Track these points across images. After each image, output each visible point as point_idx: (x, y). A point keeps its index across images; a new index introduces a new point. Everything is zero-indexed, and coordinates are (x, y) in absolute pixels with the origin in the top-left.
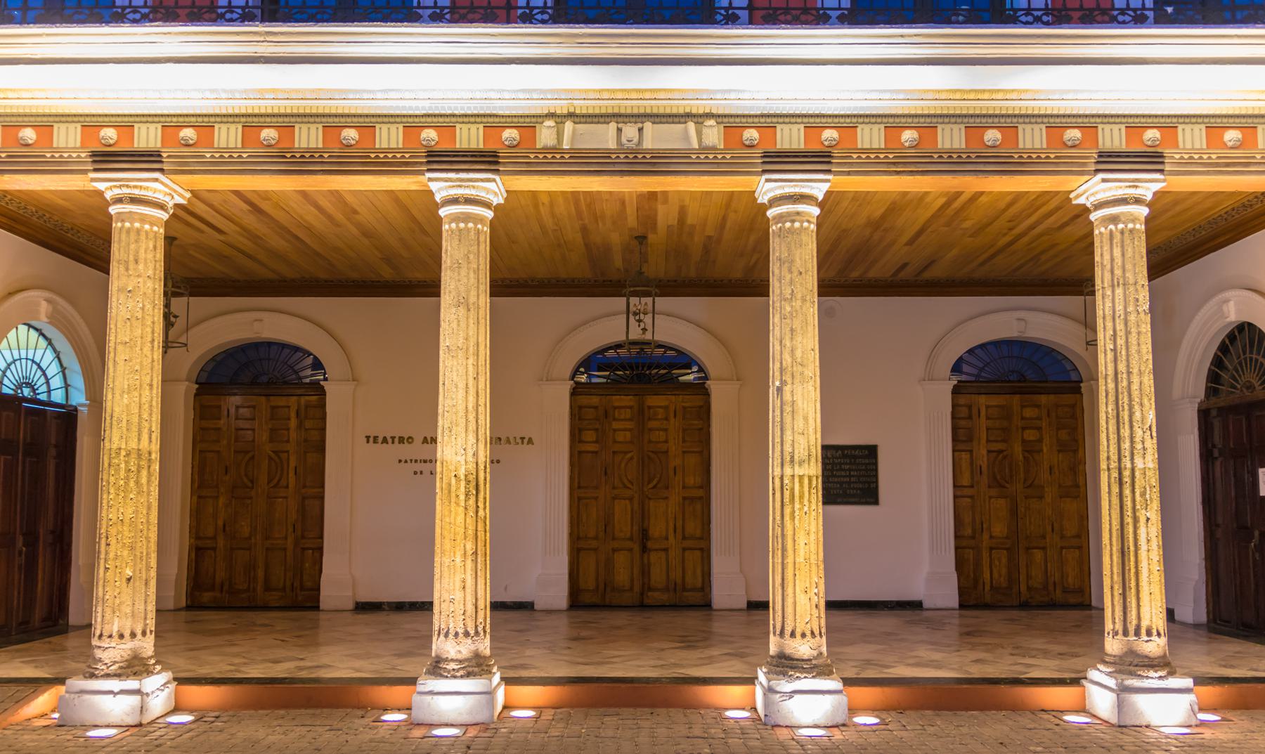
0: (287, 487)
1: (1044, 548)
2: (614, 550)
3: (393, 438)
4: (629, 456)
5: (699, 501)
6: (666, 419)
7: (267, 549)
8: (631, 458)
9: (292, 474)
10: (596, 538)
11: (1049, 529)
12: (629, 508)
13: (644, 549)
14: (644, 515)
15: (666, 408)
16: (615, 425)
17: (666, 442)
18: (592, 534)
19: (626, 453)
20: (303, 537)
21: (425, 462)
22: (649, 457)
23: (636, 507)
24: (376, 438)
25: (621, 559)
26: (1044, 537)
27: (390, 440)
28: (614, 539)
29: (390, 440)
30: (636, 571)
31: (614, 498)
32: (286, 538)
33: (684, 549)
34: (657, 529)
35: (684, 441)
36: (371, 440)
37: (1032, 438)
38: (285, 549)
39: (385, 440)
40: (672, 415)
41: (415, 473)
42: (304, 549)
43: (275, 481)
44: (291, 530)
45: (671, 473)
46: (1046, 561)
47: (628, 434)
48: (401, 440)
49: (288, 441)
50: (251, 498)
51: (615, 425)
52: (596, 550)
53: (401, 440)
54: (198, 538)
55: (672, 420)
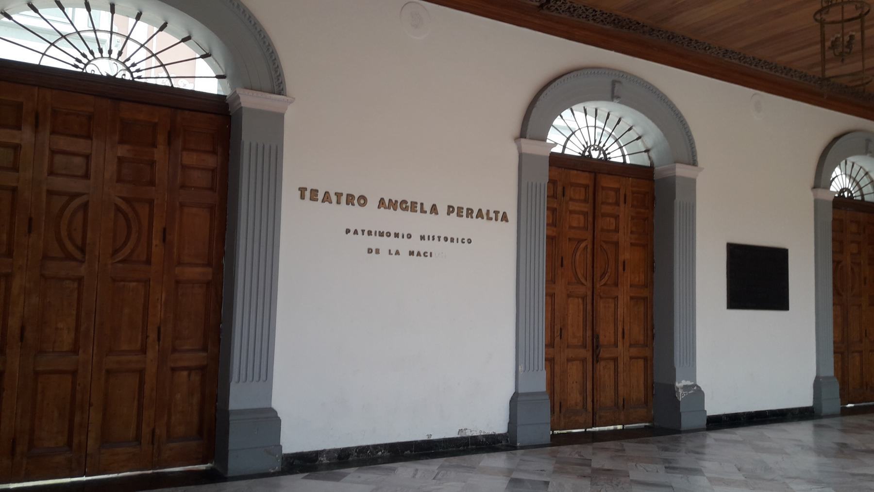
0: (148, 262)
1: (861, 352)
2: (568, 360)
3: (339, 195)
4: (583, 245)
6: (617, 204)
7: (108, 372)
11: (864, 335)
13: (596, 358)
15: (617, 191)
16: (573, 206)
17: (617, 230)
19: (580, 241)
20: (174, 350)
21: (381, 234)
23: (589, 307)
26: (861, 341)
27: (334, 199)
31: (569, 296)
32: (144, 351)
34: (606, 335)
35: (632, 232)
36: (308, 194)
38: (141, 372)
39: (327, 198)
41: (370, 251)
42: (173, 370)
43: (126, 251)
44: (153, 336)
45: (621, 268)
47: (582, 217)
48: (350, 199)
49: (152, 183)
53: (350, 199)
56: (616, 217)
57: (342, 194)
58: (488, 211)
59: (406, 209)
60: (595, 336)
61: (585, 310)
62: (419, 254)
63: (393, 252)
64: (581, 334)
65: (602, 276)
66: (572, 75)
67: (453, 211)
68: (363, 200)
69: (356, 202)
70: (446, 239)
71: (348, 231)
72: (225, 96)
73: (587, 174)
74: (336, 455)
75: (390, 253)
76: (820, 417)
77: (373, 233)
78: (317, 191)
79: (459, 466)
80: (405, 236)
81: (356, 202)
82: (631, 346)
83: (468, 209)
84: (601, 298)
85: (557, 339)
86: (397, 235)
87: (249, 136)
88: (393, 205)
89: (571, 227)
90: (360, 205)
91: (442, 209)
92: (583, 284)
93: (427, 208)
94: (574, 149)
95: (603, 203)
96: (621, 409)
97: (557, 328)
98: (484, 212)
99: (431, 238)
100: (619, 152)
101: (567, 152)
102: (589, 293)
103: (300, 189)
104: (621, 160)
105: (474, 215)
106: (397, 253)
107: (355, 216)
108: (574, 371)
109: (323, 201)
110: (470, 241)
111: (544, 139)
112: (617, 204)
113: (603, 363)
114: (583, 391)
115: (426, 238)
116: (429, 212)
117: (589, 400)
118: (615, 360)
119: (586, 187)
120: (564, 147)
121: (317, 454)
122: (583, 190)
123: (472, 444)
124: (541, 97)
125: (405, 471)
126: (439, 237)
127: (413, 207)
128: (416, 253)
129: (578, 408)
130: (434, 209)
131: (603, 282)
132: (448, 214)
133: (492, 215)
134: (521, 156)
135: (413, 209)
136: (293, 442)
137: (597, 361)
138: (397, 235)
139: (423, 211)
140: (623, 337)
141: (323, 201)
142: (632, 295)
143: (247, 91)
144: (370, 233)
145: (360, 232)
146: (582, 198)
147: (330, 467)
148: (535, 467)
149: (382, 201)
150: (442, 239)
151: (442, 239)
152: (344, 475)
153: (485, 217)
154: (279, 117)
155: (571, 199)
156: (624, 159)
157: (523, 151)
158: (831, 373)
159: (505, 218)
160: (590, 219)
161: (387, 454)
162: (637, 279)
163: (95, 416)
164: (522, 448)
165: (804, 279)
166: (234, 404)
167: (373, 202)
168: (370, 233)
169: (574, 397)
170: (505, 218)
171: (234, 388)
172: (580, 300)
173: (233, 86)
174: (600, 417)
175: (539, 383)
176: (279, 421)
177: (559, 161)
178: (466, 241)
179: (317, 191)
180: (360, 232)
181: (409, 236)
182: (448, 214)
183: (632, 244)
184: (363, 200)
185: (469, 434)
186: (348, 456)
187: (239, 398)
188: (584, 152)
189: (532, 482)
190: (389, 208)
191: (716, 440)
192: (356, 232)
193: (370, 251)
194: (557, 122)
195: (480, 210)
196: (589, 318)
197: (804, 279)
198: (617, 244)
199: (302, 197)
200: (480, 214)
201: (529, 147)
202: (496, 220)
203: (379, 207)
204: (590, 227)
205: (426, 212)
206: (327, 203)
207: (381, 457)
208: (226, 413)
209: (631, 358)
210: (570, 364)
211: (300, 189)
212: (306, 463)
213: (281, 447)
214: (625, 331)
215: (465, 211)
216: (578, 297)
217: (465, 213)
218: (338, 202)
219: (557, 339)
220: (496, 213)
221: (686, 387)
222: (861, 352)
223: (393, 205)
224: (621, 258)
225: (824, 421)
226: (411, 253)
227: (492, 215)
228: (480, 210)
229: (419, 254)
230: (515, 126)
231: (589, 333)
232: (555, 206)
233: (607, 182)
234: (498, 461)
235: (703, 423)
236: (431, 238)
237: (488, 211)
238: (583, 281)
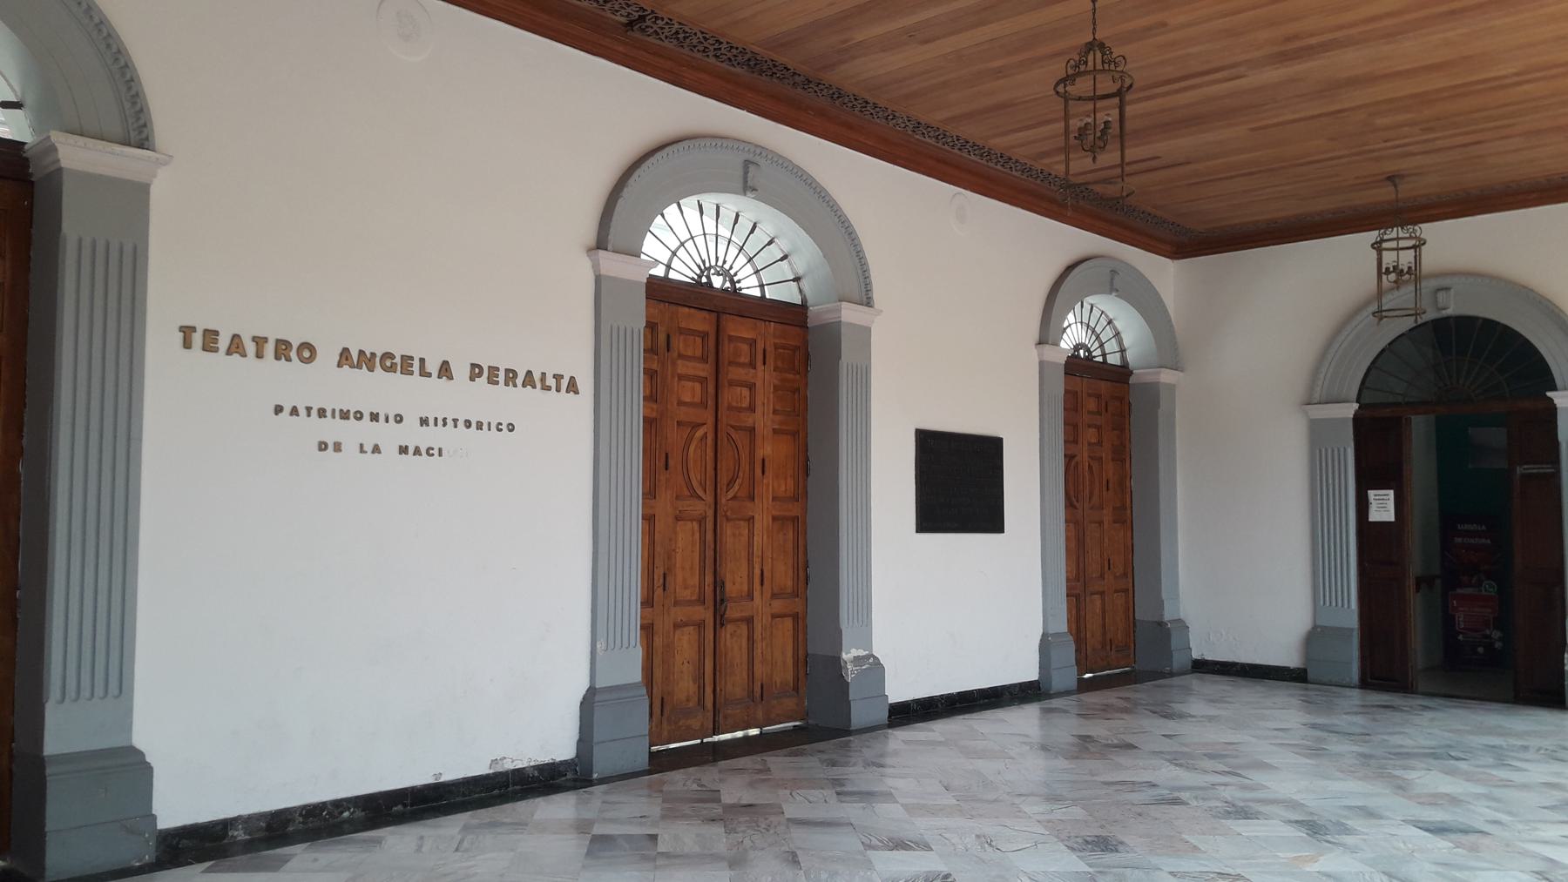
1: (1102, 593)
2: (676, 626)
3: (260, 342)
4: (699, 433)
6: (752, 365)
13: (720, 620)
16: (683, 368)
17: (752, 408)
21: (345, 415)
23: (710, 536)
24: (210, 338)
26: (1102, 577)
27: (251, 348)
28: (676, 603)
31: (678, 519)
34: (736, 582)
35: (775, 412)
36: (197, 338)
37: (1093, 440)
39: (236, 346)
45: (758, 471)
46: (1104, 612)
47: (698, 386)
48: (283, 349)
53: (283, 349)
56: (751, 387)
57: (265, 340)
58: (544, 374)
59: (392, 369)
60: (719, 584)
61: (703, 542)
62: (417, 452)
63: (369, 448)
64: (696, 580)
66: (685, 144)
67: (480, 375)
68: (308, 352)
69: (293, 354)
70: (468, 424)
71: (278, 409)
72: (19, 145)
73: (704, 314)
74: (263, 824)
75: (362, 450)
76: (1048, 696)
77: (329, 414)
78: (216, 333)
79: (494, 825)
80: (391, 419)
81: (293, 354)
82: (774, 596)
83: (507, 371)
84: (728, 520)
85: (659, 592)
86: (374, 417)
87: (77, 224)
88: (366, 361)
89: (681, 403)
90: (303, 360)
91: (461, 371)
93: (433, 367)
94: (683, 272)
95: (731, 363)
96: (758, 700)
97: (659, 572)
99: (440, 422)
100: (753, 281)
101: (673, 275)
102: (710, 513)
103: (183, 329)
104: (756, 292)
105: (519, 381)
106: (376, 449)
107: (293, 382)
108: (686, 642)
109: (229, 353)
110: (511, 428)
111: (636, 253)
112: (752, 365)
113: (730, 628)
114: (699, 678)
115: (431, 422)
116: (435, 374)
117: (709, 690)
118: (749, 621)
120: (668, 267)
121: (227, 824)
122: (699, 340)
123: (514, 784)
124: (631, 181)
125: (399, 841)
126: (455, 421)
127: (406, 365)
128: (411, 450)
130: (445, 370)
131: (731, 494)
132: (472, 379)
133: (551, 382)
134: (598, 280)
138: (374, 417)
139: (424, 373)
141: (229, 353)
143: (73, 139)
144: (322, 413)
145: (302, 412)
146: (698, 353)
147: (251, 846)
148: (627, 811)
149: (345, 353)
150: (461, 424)
151: (461, 424)
152: (285, 860)
153: (539, 385)
154: (139, 193)
155: (680, 356)
156: (763, 292)
157: (603, 272)
158: (1064, 628)
159: (573, 387)
160: (711, 389)
161: (359, 814)
164: (602, 781)
165: (1026, 485)
166: (53, 745)
167: (328, 355)
168: (322, 413)
169: (685, 687)
170: (573, 387)
171: (54, 716)
173: (39, 124)
174: (725, 717)
175: (629, 668)
176: (148, 769)
177: (660, 291)
178: (504, 427)
179: (216, 333)
180: (302, 412)
181: (399, 419)
182: (472, 379)
184: (308, 352)
185: (509, 766)
186: (288, 821)
187: (64, 730)
188: (700, 277)
189: (629, 838)
190: (359, 366)
193: (323, 446)
195: (529, 373)
196: (710, 553)
197: (1026, 485)
198: (752, 430)
199: (187, 344)
200: (529, 380)
201: (612, 264)
202: (558, 390)
203: (339, 365)
204: (711, 403)
205: (429, 375)
206: (236, 356)
207: (349, 821)
208: (38, 763)
209: (774, 616)
210: (678, 632)
211: (183, 329)
213: (154, 818)
215: (502, 374)
217: (501, 378)
218: (259, 355)
219: (659, 592)
220: (558, 377)
221: (857, 660)
222: (1102, 593)
223: (366, 361)
224: (759, 454)
225: (1056, 703)
226: (403, 450)
227: (551, 382)
228: (529, 373)
229: (417, 452)
230: (586, 229)
231: (709, 579)
232: (655, 366)
233: (737, 328)
234: (559, 808)
235: (883, 715)
236: (440, 422)
237: (544, 374)
238: (701, 493)
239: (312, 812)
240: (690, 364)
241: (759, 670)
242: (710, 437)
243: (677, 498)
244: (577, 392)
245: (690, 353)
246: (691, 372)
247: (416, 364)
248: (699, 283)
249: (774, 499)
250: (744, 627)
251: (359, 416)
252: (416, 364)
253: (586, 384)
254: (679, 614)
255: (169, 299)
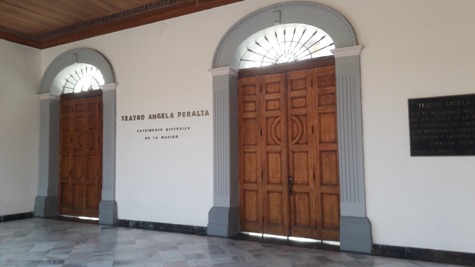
3: (134, 116)
4: (277, 120)
5: (329, 152)
6: (305, 88)
8: (279, 122)
9: (97, 142)
10: (256, 182)
12: (279, 159)
13: (291, 192)
14: (290, 166)
15: (305, 79)
16: (267, 97)
18: (253, 180)
19: (276, 118)
21: (150, 130)
22: (293, 120)
24: (126, 117)
25: (274, 199)
27: (133, 118)
28: (268, 183)
29: (133, 118)
30: (285, 209)
31: (268, 153)
32: (94, 179)
33: (322, 194)
34: (300, 177)
35: (320, 105)
39: (131, 119)
40: (309, 84)
41: (146, 138)
45: (310, 131)
47: (277, 102)
50: (81, 156)
51: (267, 97)
52: (256, 191)
54: (62, 178)
55: (309, 88)
62: (166, 137)
64: (280, 176)
65: (293, 139)
67: (180, 115)
68: (143, 117)
71: (138, 131)
82: (322, 184)
85: (260, 179)
87: (105, 100)
88: (154, 117)
91: (176, 115)
92: (278, 145)
93: (169, 115)
98: (196, 112)
100: (307, 52)
102: (284, 150)
113: (297, 196)
114: (281, 213)
118: (308, 194)
119: (278, 82)
129: (278, 222)
130: (172, 115)
131: (295, 142)
133: (200, 113)
135: (163, 117)
136: (122, 215)
137: (291, 194)
139: (167, 117)
140: (314, 179)
142: (321, 149)
144: (146, 131)
155: (267, 93)
159: (207, 113)
161: (153, 226)
162: (328, 138)
163: (84, 198)
167: (147, 117)
168: (146, 131)
170: (207, 113)
172: (278, 155)
175: (226, 203)
178: (187, 128)
183: (320, 114)
184: (143, 117)
186: (139, 224)
191: (249, 251)
192: (141, 131)
194: (321, 33)
196: (285, 166)
199: (123, 120)
200: (194, 114)
212: (125, 224)
214: (316, 175)
216: (276, 153)
217: (186, 115)
218: (135, 120)
223: (154, 117)
224: (310, 125)
231: (285, 175)
232: (255, 99)
235: (368, 249)
238: (278, 142)
239: (144, 223)
240: (273, 95)
241: (313, 215)
242: (283, 121)
243: (267, 144)
244: (209, 115)
245: (273, 91)
246: (272, 98)
247: (165, 115)
248: (276, 63)
249: (321, 142)
250: (306, 197)
251: (153, 130)
252: (165, 115)
253: (211, 112)
254: (270, 188)
255: (121, 111)
